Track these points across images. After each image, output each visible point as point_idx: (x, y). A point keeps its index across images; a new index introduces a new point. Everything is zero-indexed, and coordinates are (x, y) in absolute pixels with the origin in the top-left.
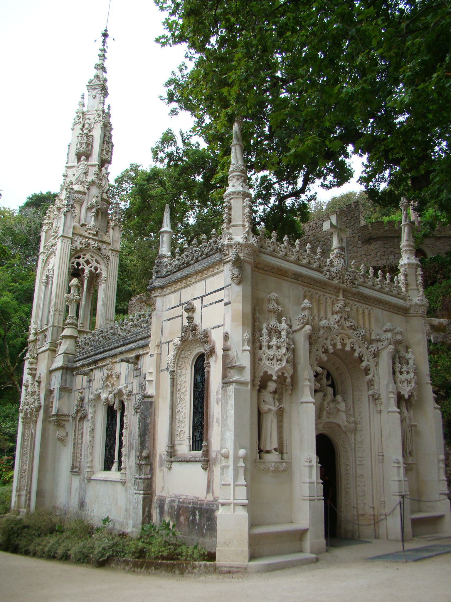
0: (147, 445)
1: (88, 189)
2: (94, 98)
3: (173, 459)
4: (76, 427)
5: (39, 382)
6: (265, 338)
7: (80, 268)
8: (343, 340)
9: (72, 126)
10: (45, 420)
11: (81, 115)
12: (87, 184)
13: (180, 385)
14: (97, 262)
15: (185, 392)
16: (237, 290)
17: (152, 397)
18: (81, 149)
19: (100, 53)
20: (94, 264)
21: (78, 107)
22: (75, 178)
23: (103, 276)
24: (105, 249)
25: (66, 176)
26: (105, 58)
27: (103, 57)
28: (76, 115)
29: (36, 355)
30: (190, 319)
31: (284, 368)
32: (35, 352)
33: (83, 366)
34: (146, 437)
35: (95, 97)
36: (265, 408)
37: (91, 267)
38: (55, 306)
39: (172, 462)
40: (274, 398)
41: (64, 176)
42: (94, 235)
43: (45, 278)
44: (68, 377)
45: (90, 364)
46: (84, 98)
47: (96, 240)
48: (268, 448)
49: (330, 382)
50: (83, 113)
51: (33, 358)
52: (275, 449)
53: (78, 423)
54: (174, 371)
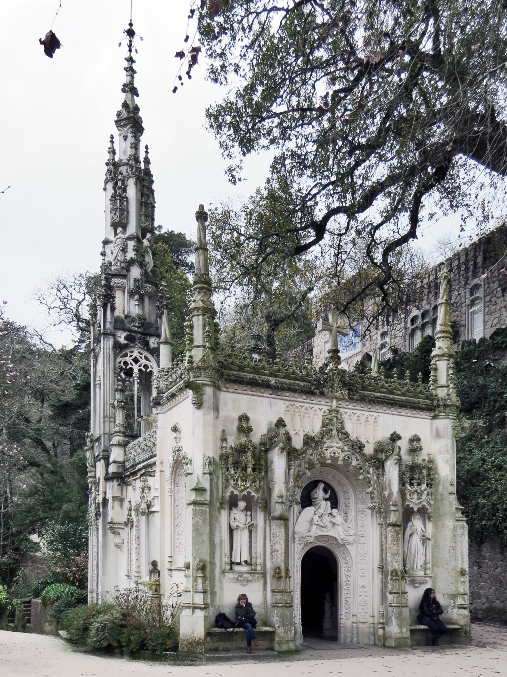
1: (128, 270)
2: (125, 140)
14: (146, 359)
18: (115, 218)
19: (126, 64)
20: (143, 362)
22: (114, 258)
26: (134, 72)
27: (131, 71)
28: (106, 168)
36: (234, 525)
37: (140, 366)
40: (246, 515)
48: (238, 561)
49: (328, 496)
52: (246, 562)
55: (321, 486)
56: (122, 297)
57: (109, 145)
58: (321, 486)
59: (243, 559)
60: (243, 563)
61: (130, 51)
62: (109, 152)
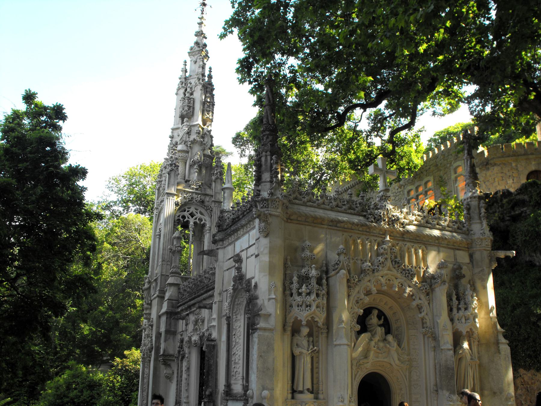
0: (210, 385)
3: (228, 398)
4: (178, 366)
5: (152, 326)
6: (295, 285)
7: (185, 220)
8: (389, 280)
9: (175, 91)
10: (156, 360)
11: (184, 80)
12: (189, 143)
13: (236, 329)
14: (201, 213)
15: (240, 336)
16: (265, 242)
17: (215, 341)
20: (198, 215)
21: (181, 73)
22: (179, 138)
23: (208, 226)
24: (208, 201)
25: (172, 137)
28: (179, 80)
29: (150, 302)
30: (239, 269)
31: (314, 313)
32: (149, 299)
33: (182, 310)
34: (210, 377)
35: (195, 62)
36: (297, 352)
37: (196, 219)
38: (163, 257)
39: (227, 400)
40: (308, 341)
41: (170, 137)
42: (197, 189)
43: (158, 231)
44: (173, 321)
45: (186, 309)
46: (186, 65)
47: (199, 194)
48: (301, 389)
49: (381, 322)
50: (186, 78)
51: (148, 304)
52: (308, 390)
53: (180, 362)
54: (230, 317)
55: (375, 312)
56: (184, 167)
57: (183, 66)
58: (375, 312)
59: (306, 387)
60: (306, 391)
61: (202, 13)
62: (182, 71)
